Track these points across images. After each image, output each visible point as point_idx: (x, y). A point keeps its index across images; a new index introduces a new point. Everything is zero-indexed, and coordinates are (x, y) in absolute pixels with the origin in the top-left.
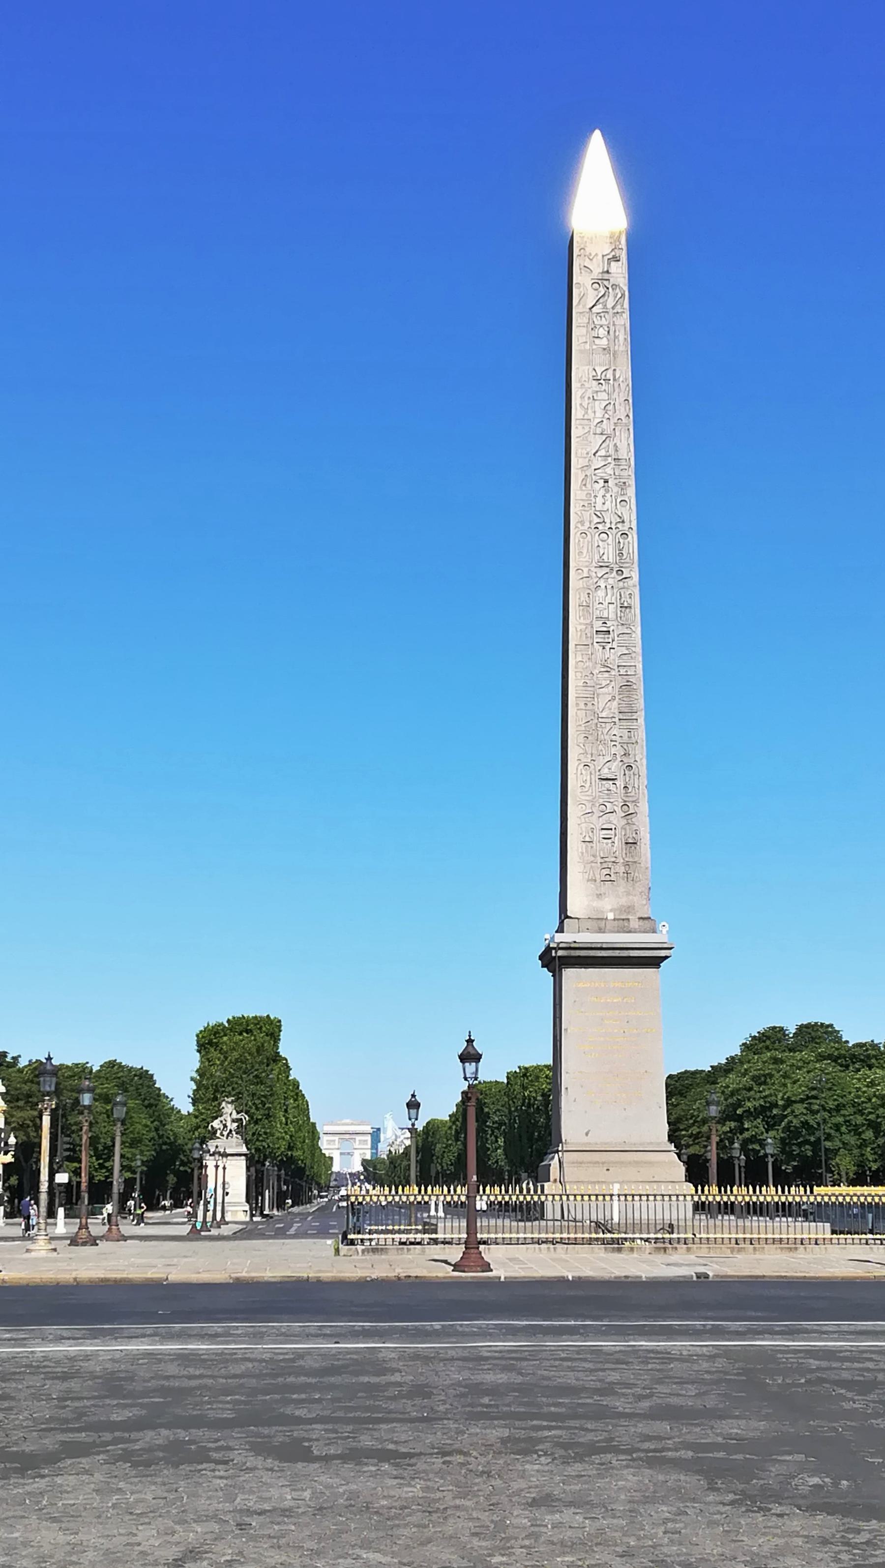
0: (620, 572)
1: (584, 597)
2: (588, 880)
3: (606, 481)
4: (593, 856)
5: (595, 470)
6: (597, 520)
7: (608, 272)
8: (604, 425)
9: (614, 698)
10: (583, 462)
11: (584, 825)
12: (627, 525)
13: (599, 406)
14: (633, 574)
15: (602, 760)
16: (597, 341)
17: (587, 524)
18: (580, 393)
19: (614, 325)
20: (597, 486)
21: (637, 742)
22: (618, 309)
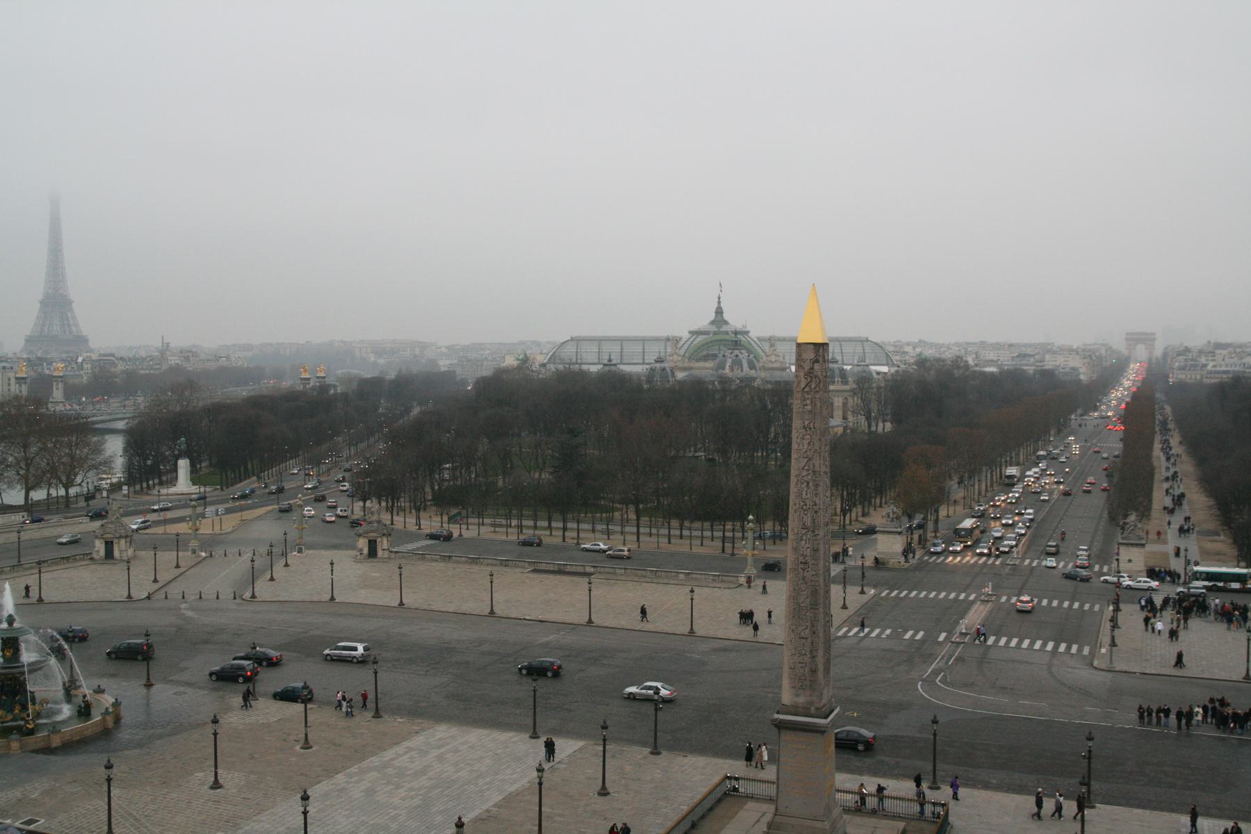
0: (813, 531)
1: (795, 544)
2: (793, 687)
3: (808, 483)
4: (796, 675)
5: (803, 477)
6: (802, 504)
7: (812, 369)
8: (808, 453)
9: (807, 597)
10: (797, 472)
11: (791, 660)
12: (818, 506)
13: (806, 442)
14: (820, 533)
15: (801, 628)
16: (806, 407)
17: (798, 506)
18: (797, 435)
19: (815, 398)
20: (804, 486)
21: (818, 621)
22: (817, 389)
